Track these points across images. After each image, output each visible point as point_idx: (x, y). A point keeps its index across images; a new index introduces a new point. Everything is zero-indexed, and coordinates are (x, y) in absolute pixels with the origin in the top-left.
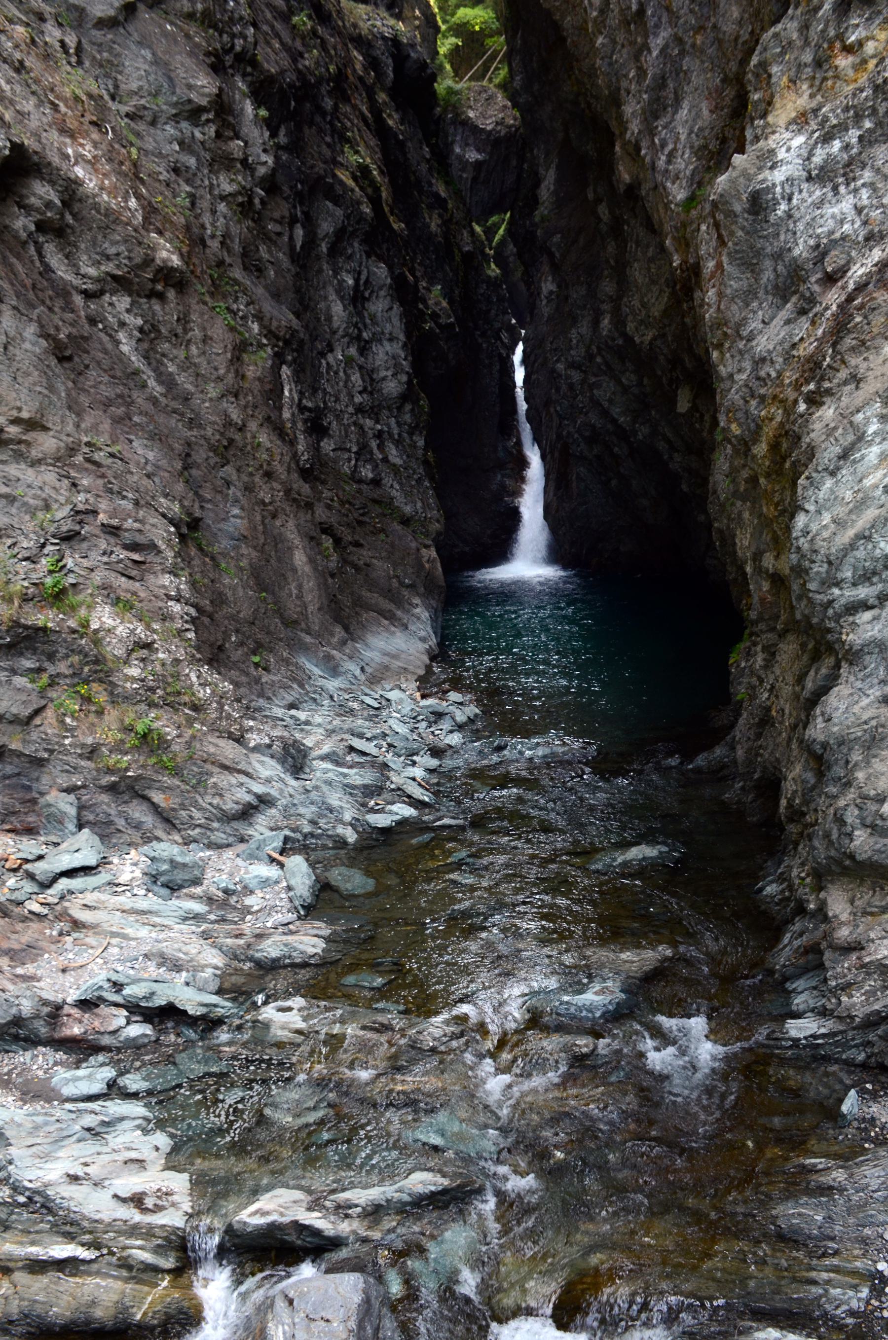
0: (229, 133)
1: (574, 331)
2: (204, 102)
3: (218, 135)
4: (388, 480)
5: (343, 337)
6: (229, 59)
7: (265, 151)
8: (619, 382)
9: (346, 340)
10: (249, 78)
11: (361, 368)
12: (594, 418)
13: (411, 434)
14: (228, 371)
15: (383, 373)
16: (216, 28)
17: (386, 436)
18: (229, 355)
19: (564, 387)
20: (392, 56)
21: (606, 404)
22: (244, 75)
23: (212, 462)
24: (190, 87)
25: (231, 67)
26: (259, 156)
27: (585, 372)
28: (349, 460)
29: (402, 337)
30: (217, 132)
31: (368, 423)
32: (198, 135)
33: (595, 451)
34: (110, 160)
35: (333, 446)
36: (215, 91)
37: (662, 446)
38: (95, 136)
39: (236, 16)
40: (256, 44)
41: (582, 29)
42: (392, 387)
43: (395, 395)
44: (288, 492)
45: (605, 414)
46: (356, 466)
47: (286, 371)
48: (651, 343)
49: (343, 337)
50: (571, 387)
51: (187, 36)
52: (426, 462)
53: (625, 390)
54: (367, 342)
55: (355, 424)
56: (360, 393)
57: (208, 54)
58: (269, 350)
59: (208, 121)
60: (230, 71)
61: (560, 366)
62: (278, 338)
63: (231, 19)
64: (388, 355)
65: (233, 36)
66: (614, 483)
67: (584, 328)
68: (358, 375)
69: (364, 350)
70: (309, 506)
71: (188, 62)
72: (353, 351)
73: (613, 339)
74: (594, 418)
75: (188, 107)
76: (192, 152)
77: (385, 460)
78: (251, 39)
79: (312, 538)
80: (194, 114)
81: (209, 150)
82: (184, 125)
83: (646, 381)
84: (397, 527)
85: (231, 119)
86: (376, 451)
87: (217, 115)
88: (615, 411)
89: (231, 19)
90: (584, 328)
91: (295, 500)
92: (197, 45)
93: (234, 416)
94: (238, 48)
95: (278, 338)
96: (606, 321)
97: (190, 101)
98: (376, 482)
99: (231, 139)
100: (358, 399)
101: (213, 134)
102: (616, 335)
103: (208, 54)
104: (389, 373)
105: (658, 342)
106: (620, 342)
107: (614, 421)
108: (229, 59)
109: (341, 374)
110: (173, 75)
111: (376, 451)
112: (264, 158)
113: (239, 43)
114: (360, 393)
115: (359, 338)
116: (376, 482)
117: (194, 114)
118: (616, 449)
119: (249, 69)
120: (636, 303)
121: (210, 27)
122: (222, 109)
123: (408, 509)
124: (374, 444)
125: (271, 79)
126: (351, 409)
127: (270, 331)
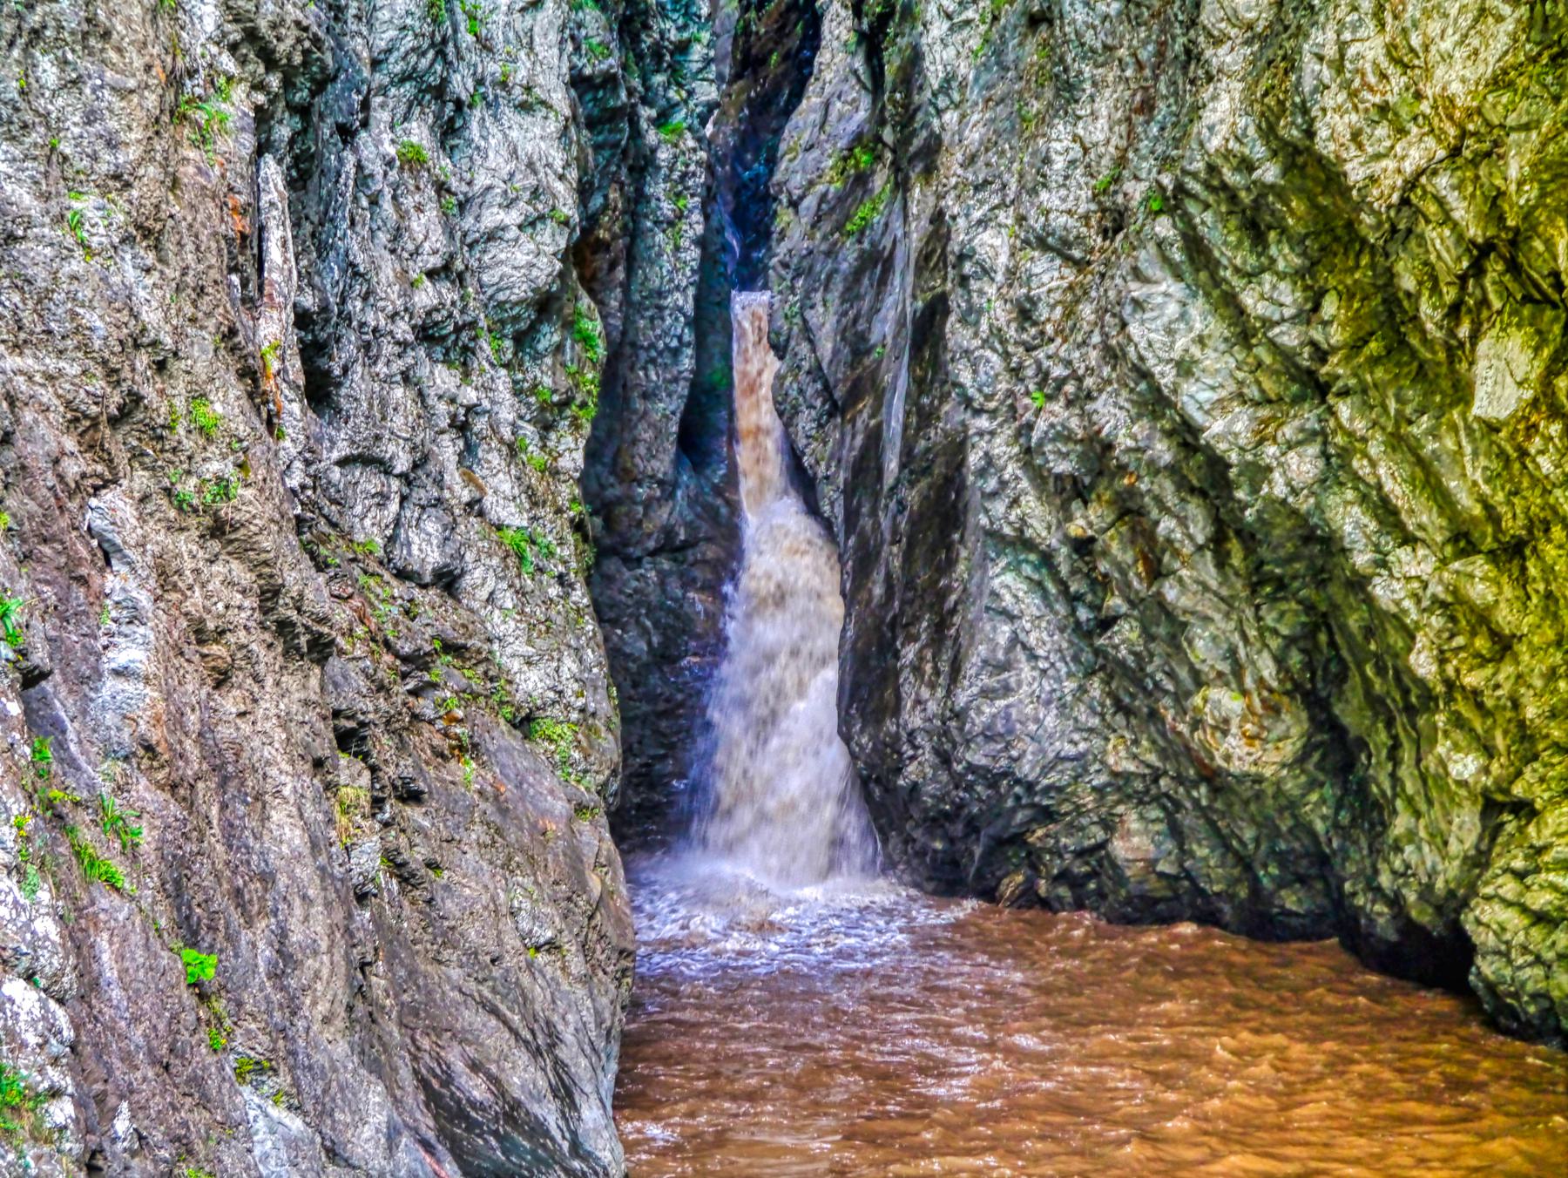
1: (1060, 128)
4: (480, 578)
5: (404, 78)
8: (1230, 305)
9: (408, 89)
11: (441, 188)
12: (1114, 416)
13: (546, 427)
14: (147, 156)
15: (492, 217)
17: (480, 424)
18: (152, 100)
19: (1001, 314)
21: (1166, 376)
23: (72, 468)
27: (1080, 265)
28: (383, 498)
29: (560, 99)
31: (443, 378)
33: (1076, 528)
35: (343, 449)
37: (1350, 520)
42: (525, 262)
43: (521, 291)
44: (270, 594)
45: (1155, 402)
46: (397, 523)
47: (273, 171)
48: (1412, 184)
49: (404, 78)
50: (1025, 313)
52: (578, 526)
53: (1244, 332)
54: (459, 104)
55: (406, 378)
56: (431, 274)
58: (239, 92)
61: (994, 245)
62: (269, 59)
64: (525, 150)
66: (1126, 635)
67: (1100, 120)
68: (432, 213)
69: (448, 132)
70: (321, 649)
72: (419, 133)
73: (1246, 165)
74: (1114, 416)
77: (474, 507)
79: (318, 764)
83: (1330, 306)
84: (502, 737)
86: (453, 477)
88: (1195, 397)
90: (1100, 120)
91: (284, 627)
93: (151, 316)
95: (269, 59)
96: (1224, 104)
98: (448, 581)
100: (426, 296)
102: (1259, 151)
104: (513, 217)
105: (1443, 182)
106: (1270, 173)
107: (1186, 435)
109: (387, 205)
111: (453, 477)
114: (431, 274)
115: (440, 92)
116: (448, 581)
118: (1166, 525)
120: (1370, 49)
123: (531, 683)
124: (448, 450)
126: (403, 329)
127: (252, 35)
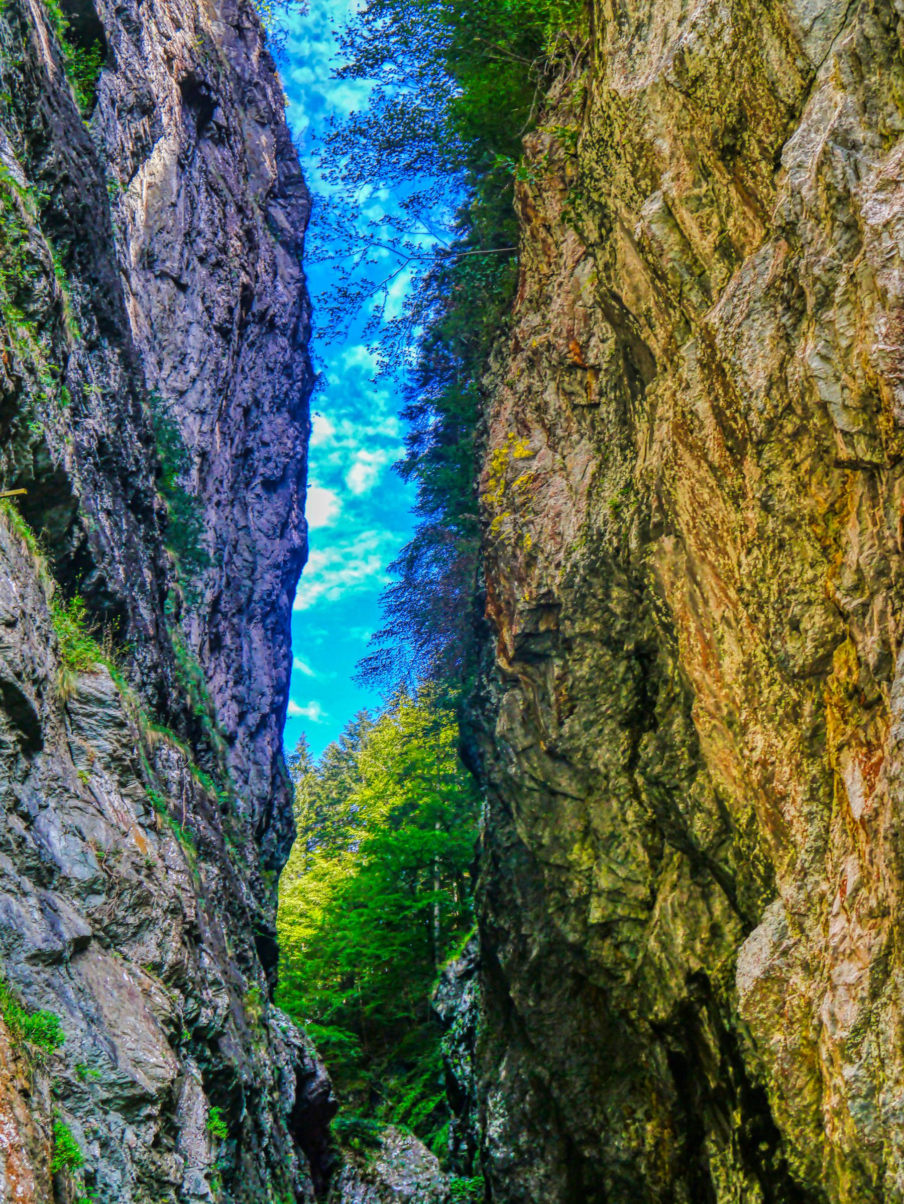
0: (167, 1141)
2: (152, 1088)
3: (157, 1143)
6: (187, 1035)
7: (208, 1177)
10: (204, 1066)
16: (183, 988)
20: (298, 1070)
22: (200, 1059)
24: (137, 1063)
25: (186, 1045)
26: (198, 1184)
30: (156, 1136)
32: (129, 1135)
34: (32, 1154)
36: (171, 1074)
38: (20, 1111)
39: (210, 977)
40: (226, 1019)
41: (806, 1056)
51: (147, 993)
57: (168, 1022)
59: (149, 1117)
60: (184, 1051)
63: (203, 980)
65: (202, 1003)
71: (143, 1027)
75: (127, 1093)
76: (118, 1163)
78: (221, 1011)
80: (132, 1104)
81: (137, 1163)
82: (115, 1117)
85: (175, 1119)
87: (162, 1112)
89: (203, 980)
92: (155, 1008)
94: (203, 1021)
97: (133, 1084)
99: (169, 1150)
101: (150, 1139)
103: (168, 1022)
108: (187, 1035)
110: (117, 1042)
112: (205, 1187)
113: (207, 1012)
117: (132, 1104)
119: (208, 1053)
121: (175, 986)
122: (169, 1102)
125: (229, 1072)
